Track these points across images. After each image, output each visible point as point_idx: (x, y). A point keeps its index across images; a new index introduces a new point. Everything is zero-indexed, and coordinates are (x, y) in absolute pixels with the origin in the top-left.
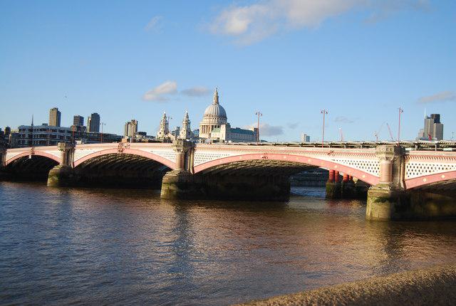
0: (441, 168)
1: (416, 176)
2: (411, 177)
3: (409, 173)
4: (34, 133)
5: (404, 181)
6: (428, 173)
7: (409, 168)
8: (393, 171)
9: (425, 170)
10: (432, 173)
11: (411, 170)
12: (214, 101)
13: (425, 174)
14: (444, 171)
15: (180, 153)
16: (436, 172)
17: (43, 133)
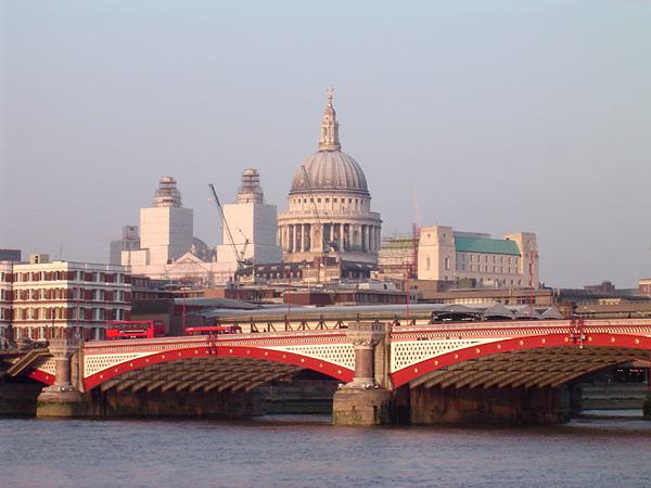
4: (19, 286)
17: (63, 284)
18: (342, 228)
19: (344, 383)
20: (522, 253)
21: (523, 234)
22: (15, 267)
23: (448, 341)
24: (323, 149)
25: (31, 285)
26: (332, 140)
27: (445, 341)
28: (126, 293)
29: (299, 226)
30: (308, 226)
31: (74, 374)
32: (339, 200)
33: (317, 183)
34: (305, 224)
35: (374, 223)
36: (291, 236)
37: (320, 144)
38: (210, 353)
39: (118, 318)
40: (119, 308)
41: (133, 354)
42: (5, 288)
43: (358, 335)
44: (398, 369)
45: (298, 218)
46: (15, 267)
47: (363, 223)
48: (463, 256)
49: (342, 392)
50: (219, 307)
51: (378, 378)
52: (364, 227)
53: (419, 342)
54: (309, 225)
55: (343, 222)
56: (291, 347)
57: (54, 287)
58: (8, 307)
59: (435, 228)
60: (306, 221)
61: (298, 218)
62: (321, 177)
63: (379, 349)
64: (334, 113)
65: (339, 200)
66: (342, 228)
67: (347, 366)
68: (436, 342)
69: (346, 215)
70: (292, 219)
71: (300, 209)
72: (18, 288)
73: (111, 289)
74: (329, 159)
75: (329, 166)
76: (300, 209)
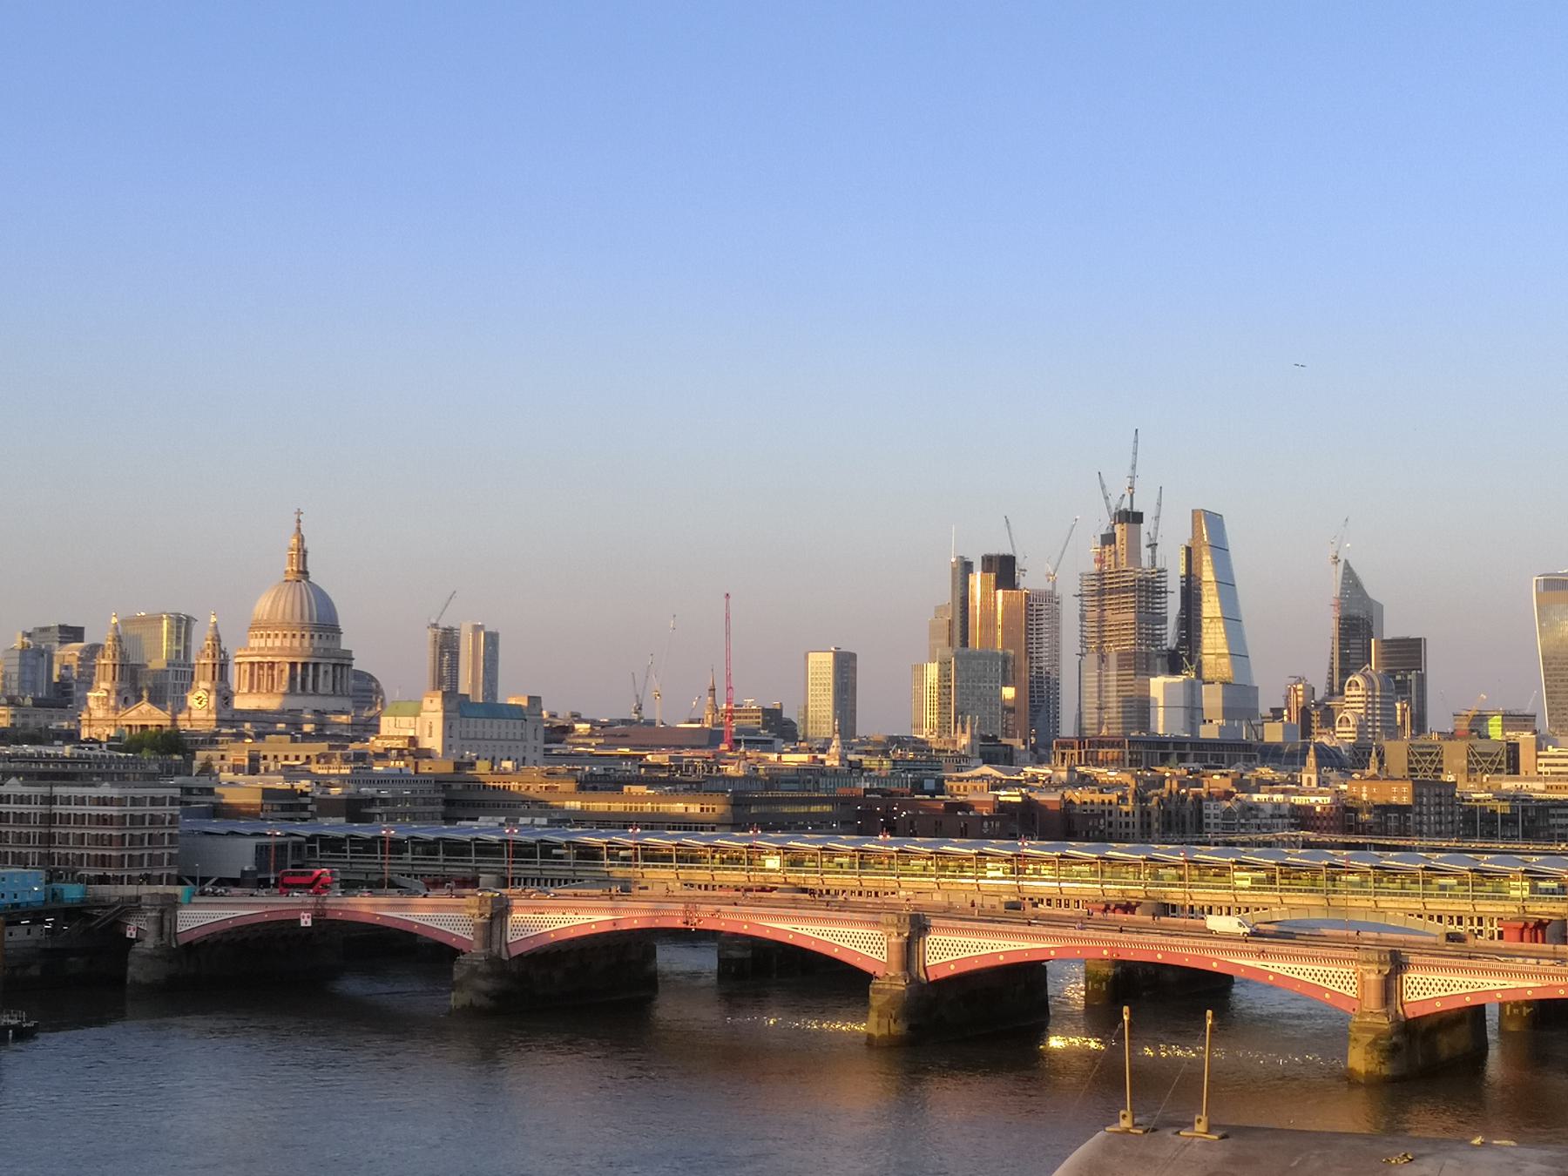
0: (1464, 985)
1: (1422, 997)
2: (1413, 999)
3: (1409, 992)
4: (58, 809)
5: (1402, 1005)
6: (1443, 994)
7: (1409, 984)
8: (1389, 989)
9: (1437, 988)
10: (1449, 993)
11: (1412, 987)
12: (288, 566)
13: (1434, 995)
14: (1470, 990)
15: (901, 940)
16: (1455, 992)
18: (311, 667)
20: (527, 717)
21: (529, 697)
22: (54, 788)
23: (564, 916)
24: (289, 578)
25: (74, 809)
27: (561, 916)
31: (166, 930)
35: (346, 662)
36: (252, 675)
37: (286, 572)
39: (166, 842)
42: (44, 812)
46: (54, 788)
47: (334, 661)
48: (476, 722)
51: (495, 948)
53: (536, 916)
54: (273, 663)
55: (314, 660)
57: (101, 813)
58: (46, 831)
61: (262, 656)
62: (288, 611)
63: (497, 921)
66: (311, 667)
68: (552, 916)
72: (58, 812)
76: (263, 645)
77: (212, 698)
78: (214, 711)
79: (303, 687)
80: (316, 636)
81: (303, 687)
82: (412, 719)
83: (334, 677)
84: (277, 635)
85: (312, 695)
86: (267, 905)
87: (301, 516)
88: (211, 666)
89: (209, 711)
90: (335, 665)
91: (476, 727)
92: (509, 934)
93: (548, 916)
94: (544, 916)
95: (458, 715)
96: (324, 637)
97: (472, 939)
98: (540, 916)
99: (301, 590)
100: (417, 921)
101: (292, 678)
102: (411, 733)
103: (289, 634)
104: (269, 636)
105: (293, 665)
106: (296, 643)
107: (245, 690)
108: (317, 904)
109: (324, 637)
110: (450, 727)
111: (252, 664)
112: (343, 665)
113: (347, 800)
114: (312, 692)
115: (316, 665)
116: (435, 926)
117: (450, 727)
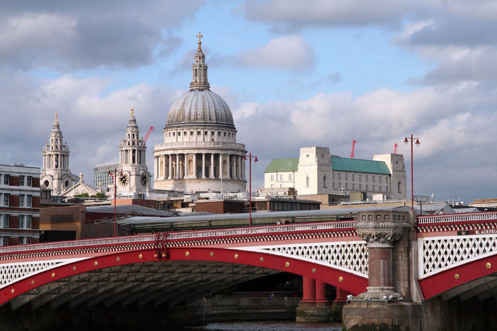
19: (354, 295)
20: (391, 172)
26: (203, 81)
28: (34, 198)
29: (174, 156)
30: (182, 156)
32: (209, 133)
33: (189, 119)
34: (180, 155)
35: (240, 153)
36: (167, 165)
38: (160, 257)
40: (26, 214)
41: (55, 261)
43: (375, 228)
44: (429, 274)
45: (174, 149)
49: (355, 306)
50: (133, 215)
51: (402, 287)
52: (231, 156)
53: (461, 237)
56: (271, 247)
59: (314, 149)
60: (180, 152)
61: (174, 149)
62: (193, 111)
64: (204, 57)
65: (209, 133)
67: (351, 271)
68: (487, 236)
69: (216, 146)
70: (168, 150)
71: (175, 140)
73: (17, 193)
74: (200, 97)
75: (200, 104)
77: (133, 178)
78: (135, 188)
79: (207, 174)
80: (216, 133)
81: (207, 174)
82: (292, 173)
83: (231, 166)
84: (185, 133)
85: (213, 180)
86: (95, 248)
87: (202, 40)
88: (131, 152)
89: (131, 189)
90: (231, 156)
91: (346, 180)
92: (422, 266)
93: (481, 237)
94: (474, 237)
95: (331, 169)
96: (222, 134)
97: (366, 276)
98: (468, 237)
99: (203, 97)
100: (289, 255)
101: (199, 169)
102: (291, 186)
103: (195, 132)
104: (179, 134)
105: (199, 156)
106: (200, 138)
107: (163, 178)
108: (157, 243)
109: (222, 134)
110: (325, 178)
111: (167, 156)
112: (237, 156)
113: (224, 202)
114: (214, 177)
115: (217, 156)
116: (313, 261)
117: (325, 178)
